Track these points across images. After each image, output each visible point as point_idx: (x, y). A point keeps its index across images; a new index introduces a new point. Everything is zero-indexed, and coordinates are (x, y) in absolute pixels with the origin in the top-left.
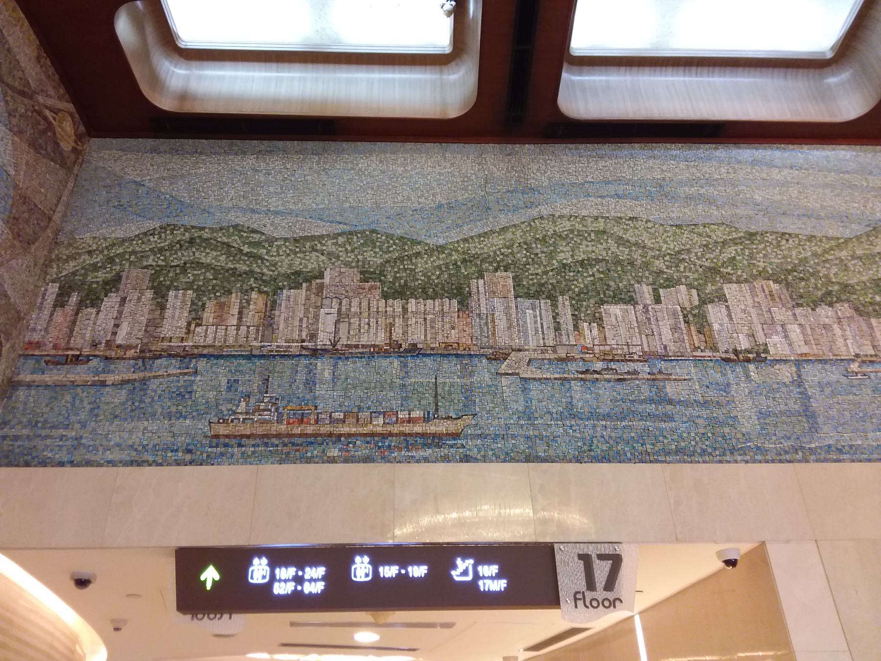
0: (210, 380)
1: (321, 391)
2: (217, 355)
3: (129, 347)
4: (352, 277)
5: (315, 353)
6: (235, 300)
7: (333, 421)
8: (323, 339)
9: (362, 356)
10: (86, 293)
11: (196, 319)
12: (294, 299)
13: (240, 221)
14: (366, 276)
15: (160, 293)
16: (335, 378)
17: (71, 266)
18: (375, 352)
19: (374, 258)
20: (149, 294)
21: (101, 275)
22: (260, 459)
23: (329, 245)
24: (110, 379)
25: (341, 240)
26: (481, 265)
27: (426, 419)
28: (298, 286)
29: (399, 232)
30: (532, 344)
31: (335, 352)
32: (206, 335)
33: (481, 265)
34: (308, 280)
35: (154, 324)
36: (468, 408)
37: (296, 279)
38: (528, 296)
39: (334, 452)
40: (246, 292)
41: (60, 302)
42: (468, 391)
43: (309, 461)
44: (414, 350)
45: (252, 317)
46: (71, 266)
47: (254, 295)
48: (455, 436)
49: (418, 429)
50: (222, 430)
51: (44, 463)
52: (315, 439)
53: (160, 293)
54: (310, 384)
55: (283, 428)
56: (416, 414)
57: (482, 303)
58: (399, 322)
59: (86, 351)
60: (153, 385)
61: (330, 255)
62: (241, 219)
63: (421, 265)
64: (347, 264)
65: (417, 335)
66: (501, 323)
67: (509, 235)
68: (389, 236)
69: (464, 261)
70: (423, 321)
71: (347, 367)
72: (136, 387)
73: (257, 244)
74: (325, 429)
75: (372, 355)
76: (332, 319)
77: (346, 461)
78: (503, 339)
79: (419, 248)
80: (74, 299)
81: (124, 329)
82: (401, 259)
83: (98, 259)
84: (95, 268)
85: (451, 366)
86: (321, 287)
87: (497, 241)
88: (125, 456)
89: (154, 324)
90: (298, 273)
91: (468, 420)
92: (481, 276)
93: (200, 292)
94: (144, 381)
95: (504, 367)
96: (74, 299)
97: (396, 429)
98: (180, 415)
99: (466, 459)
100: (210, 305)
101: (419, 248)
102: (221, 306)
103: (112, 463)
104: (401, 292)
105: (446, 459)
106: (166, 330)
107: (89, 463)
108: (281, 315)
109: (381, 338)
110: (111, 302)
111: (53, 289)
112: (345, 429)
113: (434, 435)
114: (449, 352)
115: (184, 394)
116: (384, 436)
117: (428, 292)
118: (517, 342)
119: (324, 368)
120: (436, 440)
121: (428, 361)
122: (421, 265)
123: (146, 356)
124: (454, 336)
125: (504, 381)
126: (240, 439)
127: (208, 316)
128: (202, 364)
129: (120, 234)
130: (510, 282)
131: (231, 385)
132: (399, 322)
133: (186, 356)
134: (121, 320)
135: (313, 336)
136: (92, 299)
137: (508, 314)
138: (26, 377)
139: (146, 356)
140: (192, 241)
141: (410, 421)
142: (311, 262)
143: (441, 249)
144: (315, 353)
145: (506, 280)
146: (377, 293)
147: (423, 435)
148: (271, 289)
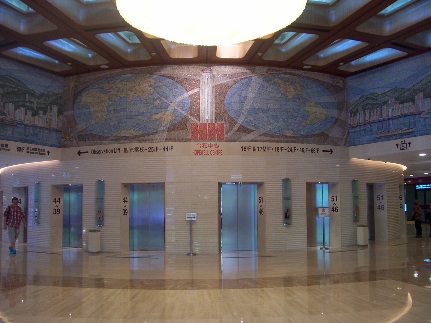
0: (375, 126)
1: (391, 126)
2: (375, 122)
3: (362, 123)
4: (394, 100)
5: (389, 119)
6: (375, 110)
7: (393, 132)
8: (390, 116)
9: (397, 118)
10: (354, 113)
11: (370, 116)
12: (384, 107)
13: (373, 92)
14: (396, 100)
15: (364, 110)
16: (393, 124)
17: (351, 109)
18: (399, 117)
19: (397, 95)
20: (363, 112)
21: (355, 109)
22: (384, 140)
23: (389, 94)
24: (361, 129)
25: (391, 92)
26: (416, 92)
27: (408, 129)
28: (384, 105)
29: (401, 87)
30: (426, 109)
31: (393, 118)
32: (373, 119)
33: (416, 92)
34: (386, 103)
35: (365, 118)
36: (415, 126)
37: (385, 103)
38: (426, 98)
39: (394, 138)
40: (377, 108)
41: (351, 116)
42: (415, 122)
43: (391, 140)
44: (405, 116)
45: (379, 113)
46: (351, 109)
47: (378, 108)
48: (413, 132)
49: (407, 131)
50: (378, 136)
51: (356, 145)
52: (391, 136)
53: (364, 110)
54: (389, 125)
55: (386, 134)
56: (406, 128)
57: (417, 101)
58: (402, 109)
59: (357, 125)
60: (367, 129)
61: (389, 96)
62: (373, 91)
63: (406, 94)
64: (392, 97)
65: (406, 112)
66: (421, 106)
67: (422, 82)
68: (399, 88)
69: (414, 92)
70: (408, 108)
71: (395, 121)
72: (365, 130)
73: (376, 97)
74: (393, 134)
75: (398, 118)
76: (391, 111)
77: (396, 139)
78: (421, 110)
79: (405, 90)
80: (353, 115)
81: (361, 120)
82: (401, 94)
83: (354, 106)
84: (354, 108)
85: (412, 117)
86: (388, 104)
87: (420, 84)
88: (366, 142)
89: (365, 118)
90: (384, 102)
91: (415, 128)
92: (417, 95)
93: (370, 109)
94: (365, 129)
95: (421, 116)
96: (353, 115)
97: (403, 132)
98: (372, 134)
99: (415, 136)
100: (372, 112)
101: (405, 90)
102: (374, 112)
103: (365, 144)
104: (402, 103)
105: (411, 137)
106: (367, 119)
107: (361, 144)
108: (383, 112)
109: (399, 114)
110: (358, 114)
111: (349, 113)
112: (395, 133)
113: (410, 132)
114: (411, 115)
115: (371, 130)
116: (401, 134)
117: (407, 101)
118: (423, 110)
119: (391, 122)
120: (409, 133)
121: (408, 117)
122: (406, 94)
123: (365, 124)
124: (412, 111)
125: (421, 119)
126: (380, 137)
127: (372, 114)
128: (373, 124)
129: (356, 100)
130: (422, 95)
131: (378, 128)
132: (402, 109)
133: (370, 123)
134: (359, 118)
135: (388, 115)
136: (355, 115)
137: (422, 103)
138: (350, 131)
139: (365, 124)
140: (366, 99)
141: (406, 130)
142: (386, 98)
143: (409, 89)
144: (389, 119)
145: (421, 94)
146: (398, 103)
147: (408, 133)
148: (381, 106)
